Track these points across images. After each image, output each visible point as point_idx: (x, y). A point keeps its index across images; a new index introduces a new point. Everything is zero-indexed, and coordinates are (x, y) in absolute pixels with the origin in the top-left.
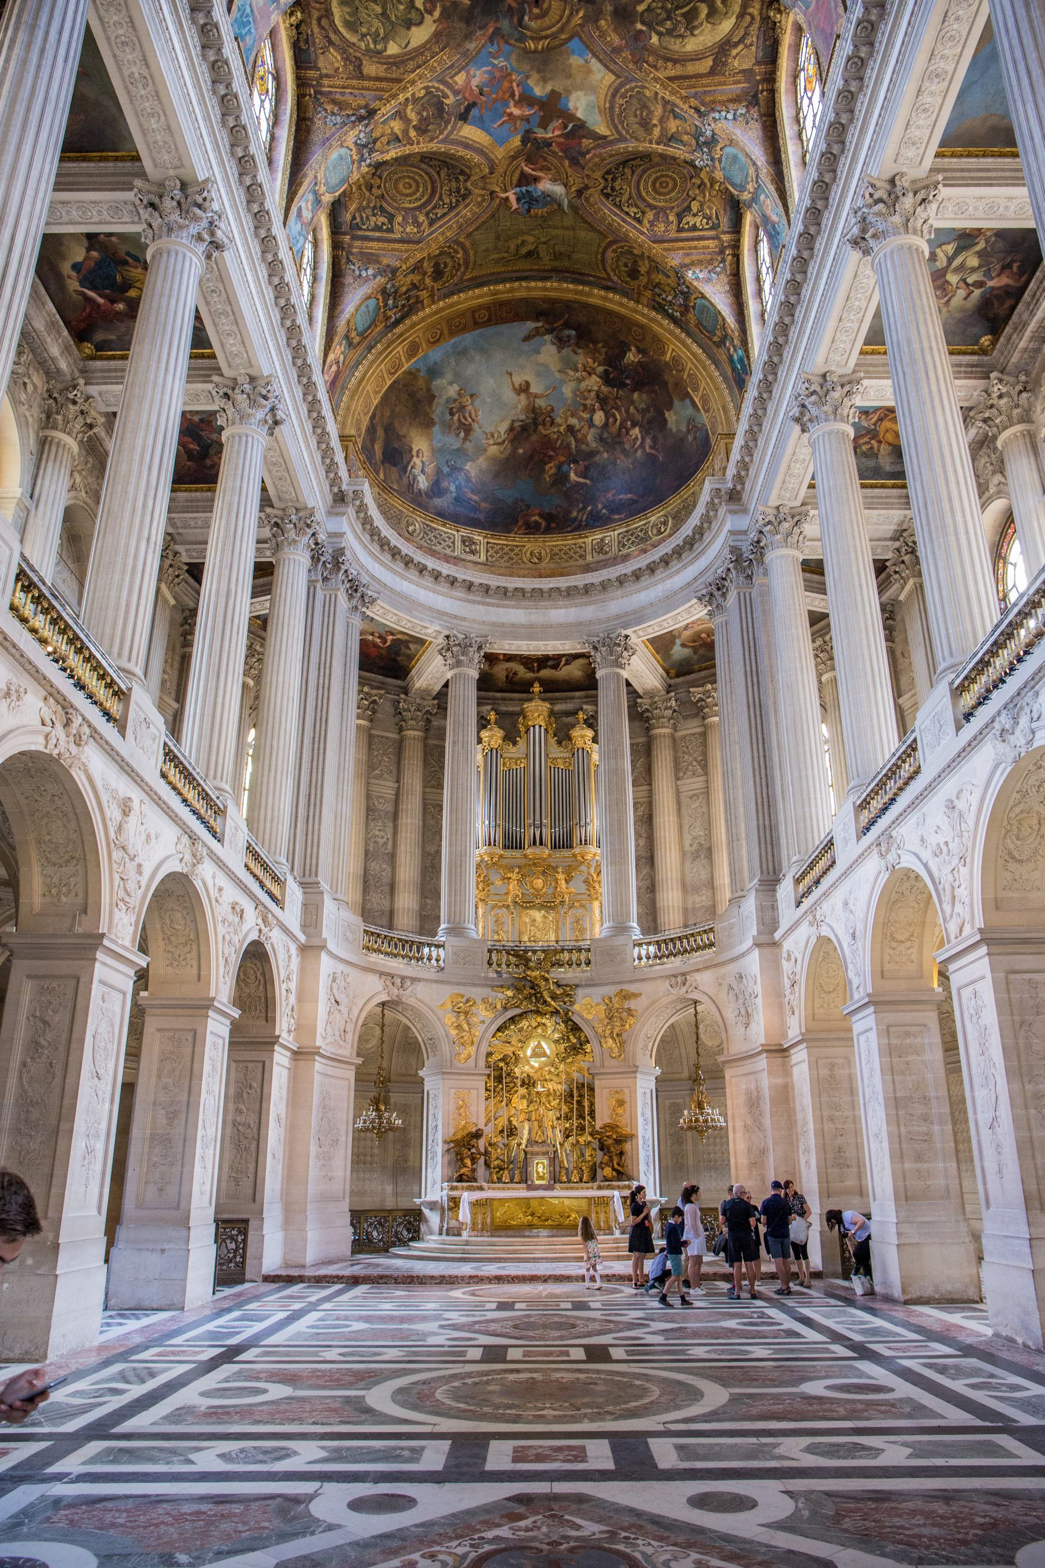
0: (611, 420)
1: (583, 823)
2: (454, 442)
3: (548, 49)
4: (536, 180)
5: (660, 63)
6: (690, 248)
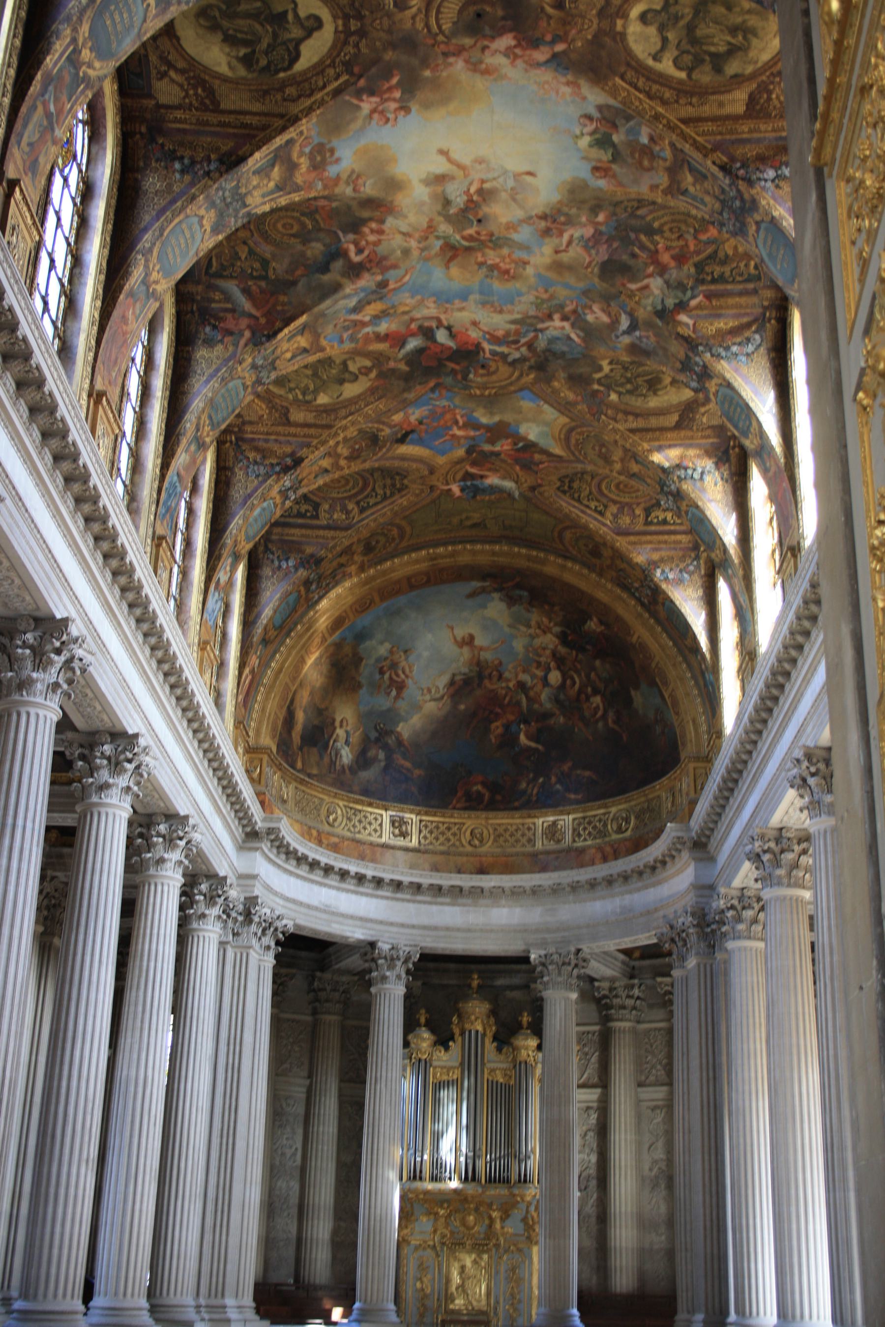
0: (568, 682)
2: (383, 702)
4: (482, 477)
5: (620, 416)
6: (659, 542)
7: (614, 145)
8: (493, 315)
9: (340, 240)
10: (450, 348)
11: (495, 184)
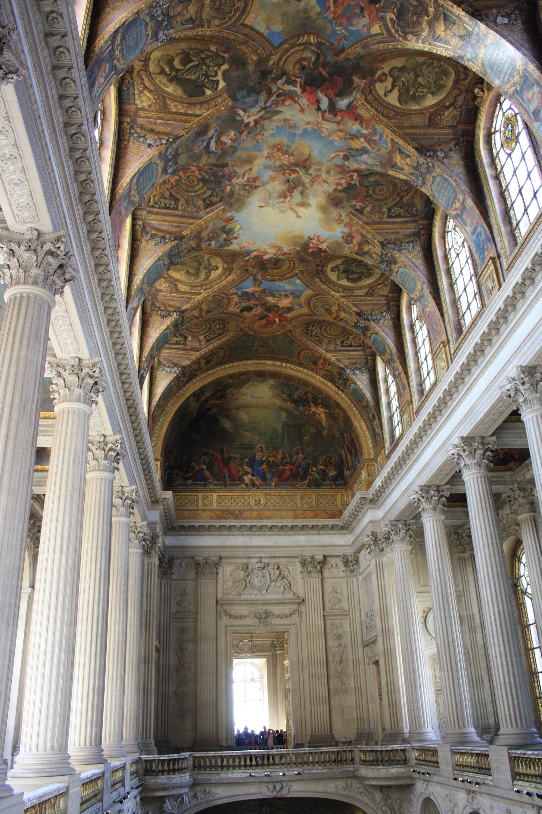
3: (299, 36)
7: (225, 232)
8: (291, 118)
9: (359, 182)
10: (321, 91)
11: (278, 201)
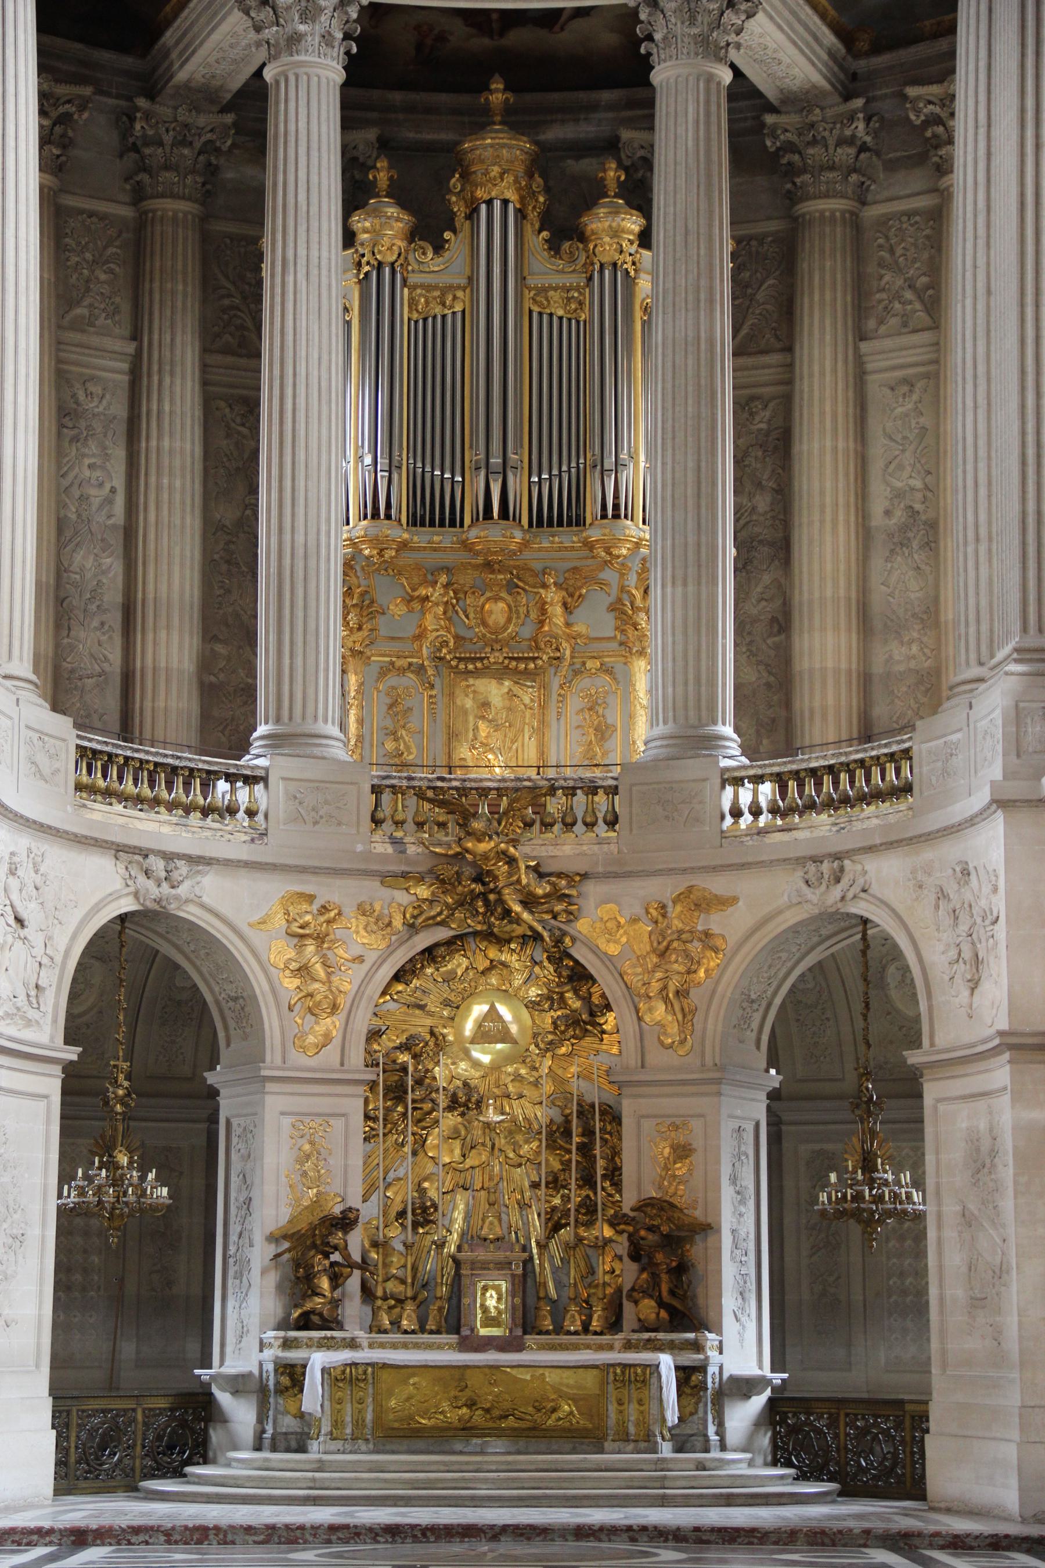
1: (610, 462)
